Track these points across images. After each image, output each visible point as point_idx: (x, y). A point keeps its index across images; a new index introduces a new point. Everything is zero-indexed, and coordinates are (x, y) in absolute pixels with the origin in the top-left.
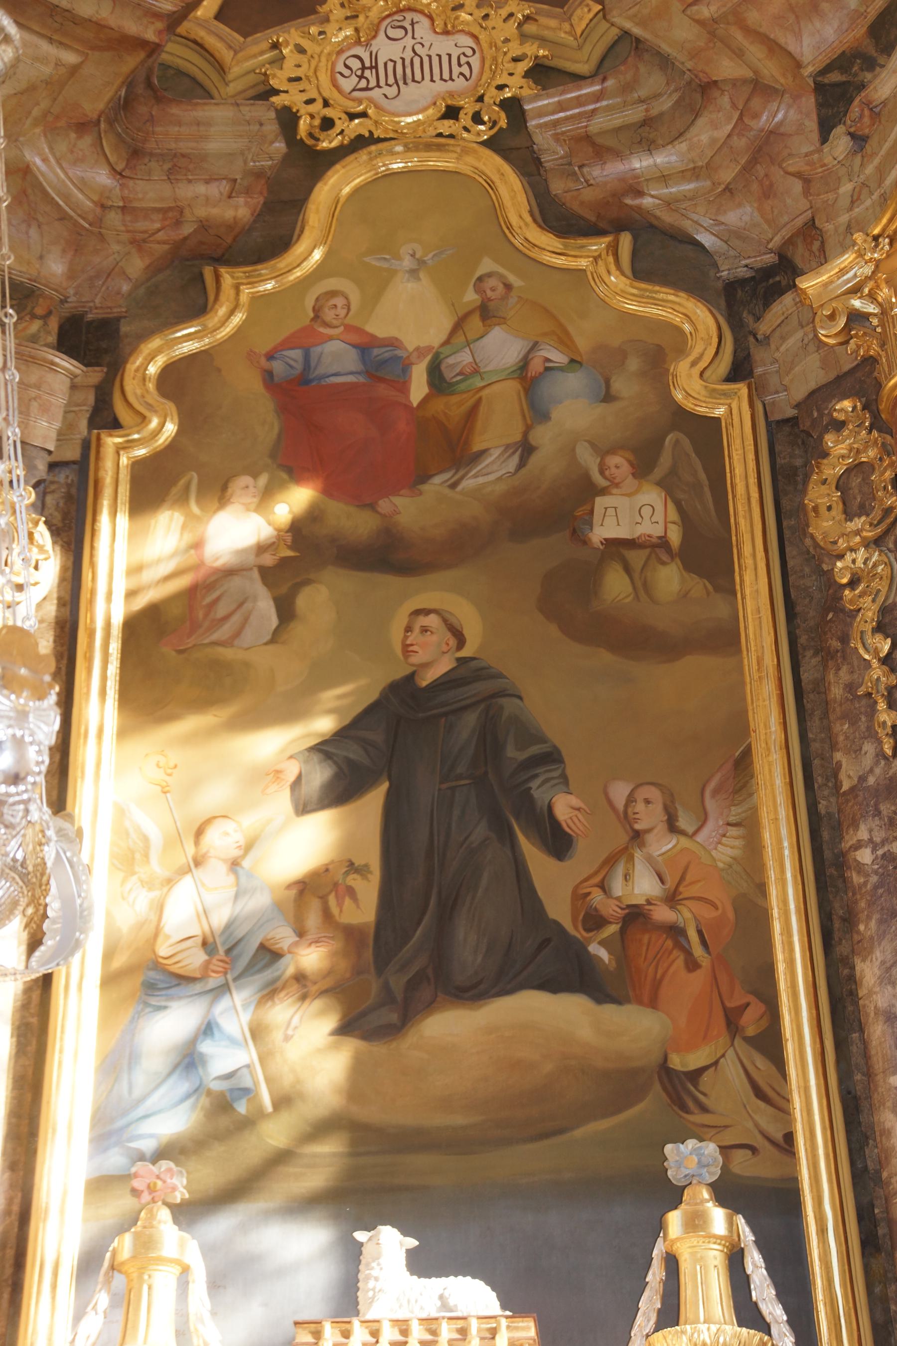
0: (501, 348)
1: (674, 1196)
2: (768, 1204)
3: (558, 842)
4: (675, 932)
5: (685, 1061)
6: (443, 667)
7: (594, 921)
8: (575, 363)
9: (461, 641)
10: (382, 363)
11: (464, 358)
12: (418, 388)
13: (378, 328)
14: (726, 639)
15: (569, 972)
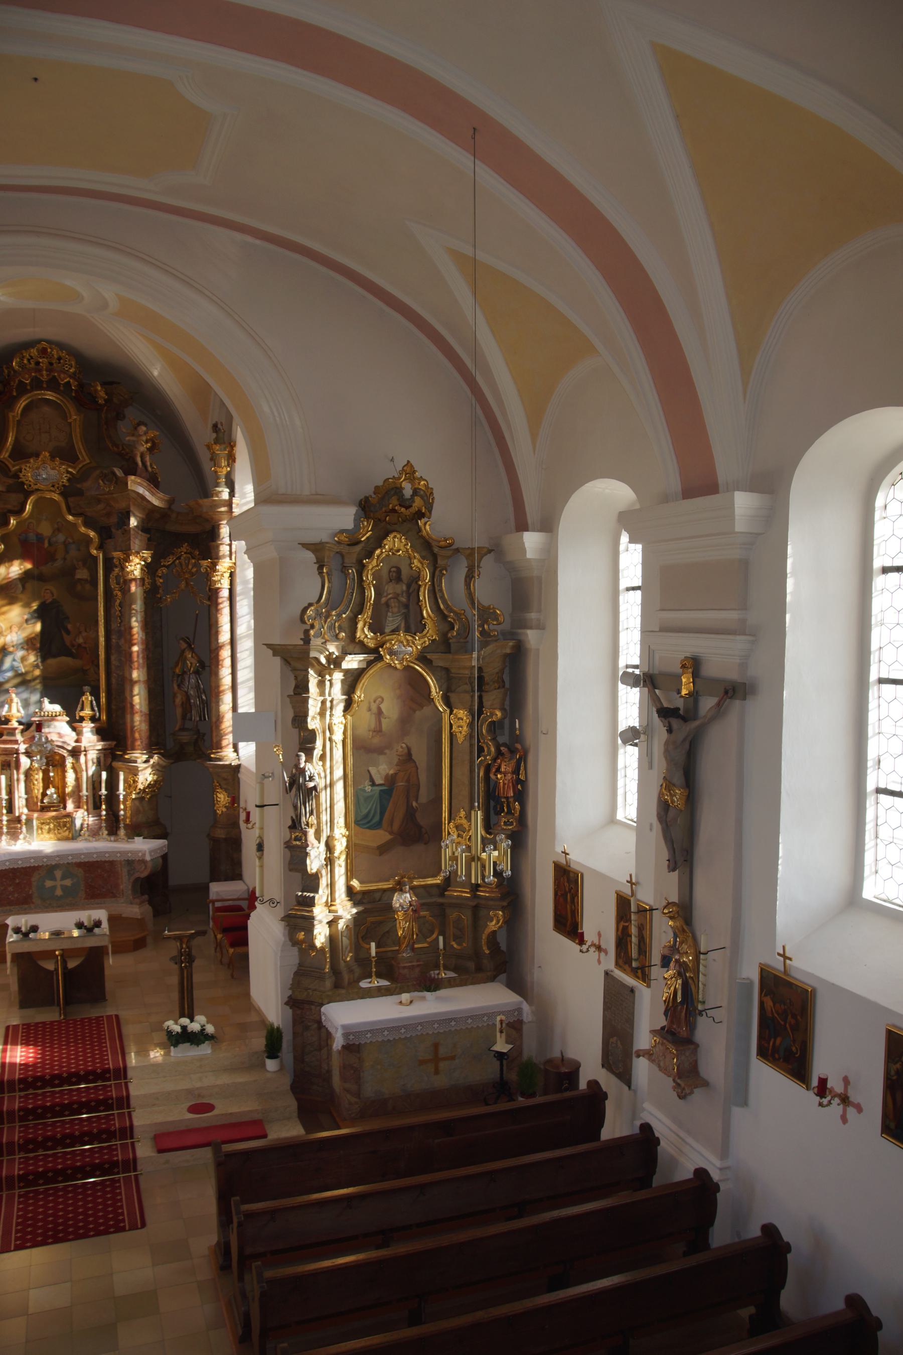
0: (61, 538)
1: (83, 694)
2: (96, 694)
4: (85, 648)
6: (50, 600)
7: (73, 646)
8: (74, 542)
9: (53, 595)
10: (40, 538)
11: (54, 539)
12: (46, 545)
13: (39, 531)
14: (96, 599)
15: (69, 654)
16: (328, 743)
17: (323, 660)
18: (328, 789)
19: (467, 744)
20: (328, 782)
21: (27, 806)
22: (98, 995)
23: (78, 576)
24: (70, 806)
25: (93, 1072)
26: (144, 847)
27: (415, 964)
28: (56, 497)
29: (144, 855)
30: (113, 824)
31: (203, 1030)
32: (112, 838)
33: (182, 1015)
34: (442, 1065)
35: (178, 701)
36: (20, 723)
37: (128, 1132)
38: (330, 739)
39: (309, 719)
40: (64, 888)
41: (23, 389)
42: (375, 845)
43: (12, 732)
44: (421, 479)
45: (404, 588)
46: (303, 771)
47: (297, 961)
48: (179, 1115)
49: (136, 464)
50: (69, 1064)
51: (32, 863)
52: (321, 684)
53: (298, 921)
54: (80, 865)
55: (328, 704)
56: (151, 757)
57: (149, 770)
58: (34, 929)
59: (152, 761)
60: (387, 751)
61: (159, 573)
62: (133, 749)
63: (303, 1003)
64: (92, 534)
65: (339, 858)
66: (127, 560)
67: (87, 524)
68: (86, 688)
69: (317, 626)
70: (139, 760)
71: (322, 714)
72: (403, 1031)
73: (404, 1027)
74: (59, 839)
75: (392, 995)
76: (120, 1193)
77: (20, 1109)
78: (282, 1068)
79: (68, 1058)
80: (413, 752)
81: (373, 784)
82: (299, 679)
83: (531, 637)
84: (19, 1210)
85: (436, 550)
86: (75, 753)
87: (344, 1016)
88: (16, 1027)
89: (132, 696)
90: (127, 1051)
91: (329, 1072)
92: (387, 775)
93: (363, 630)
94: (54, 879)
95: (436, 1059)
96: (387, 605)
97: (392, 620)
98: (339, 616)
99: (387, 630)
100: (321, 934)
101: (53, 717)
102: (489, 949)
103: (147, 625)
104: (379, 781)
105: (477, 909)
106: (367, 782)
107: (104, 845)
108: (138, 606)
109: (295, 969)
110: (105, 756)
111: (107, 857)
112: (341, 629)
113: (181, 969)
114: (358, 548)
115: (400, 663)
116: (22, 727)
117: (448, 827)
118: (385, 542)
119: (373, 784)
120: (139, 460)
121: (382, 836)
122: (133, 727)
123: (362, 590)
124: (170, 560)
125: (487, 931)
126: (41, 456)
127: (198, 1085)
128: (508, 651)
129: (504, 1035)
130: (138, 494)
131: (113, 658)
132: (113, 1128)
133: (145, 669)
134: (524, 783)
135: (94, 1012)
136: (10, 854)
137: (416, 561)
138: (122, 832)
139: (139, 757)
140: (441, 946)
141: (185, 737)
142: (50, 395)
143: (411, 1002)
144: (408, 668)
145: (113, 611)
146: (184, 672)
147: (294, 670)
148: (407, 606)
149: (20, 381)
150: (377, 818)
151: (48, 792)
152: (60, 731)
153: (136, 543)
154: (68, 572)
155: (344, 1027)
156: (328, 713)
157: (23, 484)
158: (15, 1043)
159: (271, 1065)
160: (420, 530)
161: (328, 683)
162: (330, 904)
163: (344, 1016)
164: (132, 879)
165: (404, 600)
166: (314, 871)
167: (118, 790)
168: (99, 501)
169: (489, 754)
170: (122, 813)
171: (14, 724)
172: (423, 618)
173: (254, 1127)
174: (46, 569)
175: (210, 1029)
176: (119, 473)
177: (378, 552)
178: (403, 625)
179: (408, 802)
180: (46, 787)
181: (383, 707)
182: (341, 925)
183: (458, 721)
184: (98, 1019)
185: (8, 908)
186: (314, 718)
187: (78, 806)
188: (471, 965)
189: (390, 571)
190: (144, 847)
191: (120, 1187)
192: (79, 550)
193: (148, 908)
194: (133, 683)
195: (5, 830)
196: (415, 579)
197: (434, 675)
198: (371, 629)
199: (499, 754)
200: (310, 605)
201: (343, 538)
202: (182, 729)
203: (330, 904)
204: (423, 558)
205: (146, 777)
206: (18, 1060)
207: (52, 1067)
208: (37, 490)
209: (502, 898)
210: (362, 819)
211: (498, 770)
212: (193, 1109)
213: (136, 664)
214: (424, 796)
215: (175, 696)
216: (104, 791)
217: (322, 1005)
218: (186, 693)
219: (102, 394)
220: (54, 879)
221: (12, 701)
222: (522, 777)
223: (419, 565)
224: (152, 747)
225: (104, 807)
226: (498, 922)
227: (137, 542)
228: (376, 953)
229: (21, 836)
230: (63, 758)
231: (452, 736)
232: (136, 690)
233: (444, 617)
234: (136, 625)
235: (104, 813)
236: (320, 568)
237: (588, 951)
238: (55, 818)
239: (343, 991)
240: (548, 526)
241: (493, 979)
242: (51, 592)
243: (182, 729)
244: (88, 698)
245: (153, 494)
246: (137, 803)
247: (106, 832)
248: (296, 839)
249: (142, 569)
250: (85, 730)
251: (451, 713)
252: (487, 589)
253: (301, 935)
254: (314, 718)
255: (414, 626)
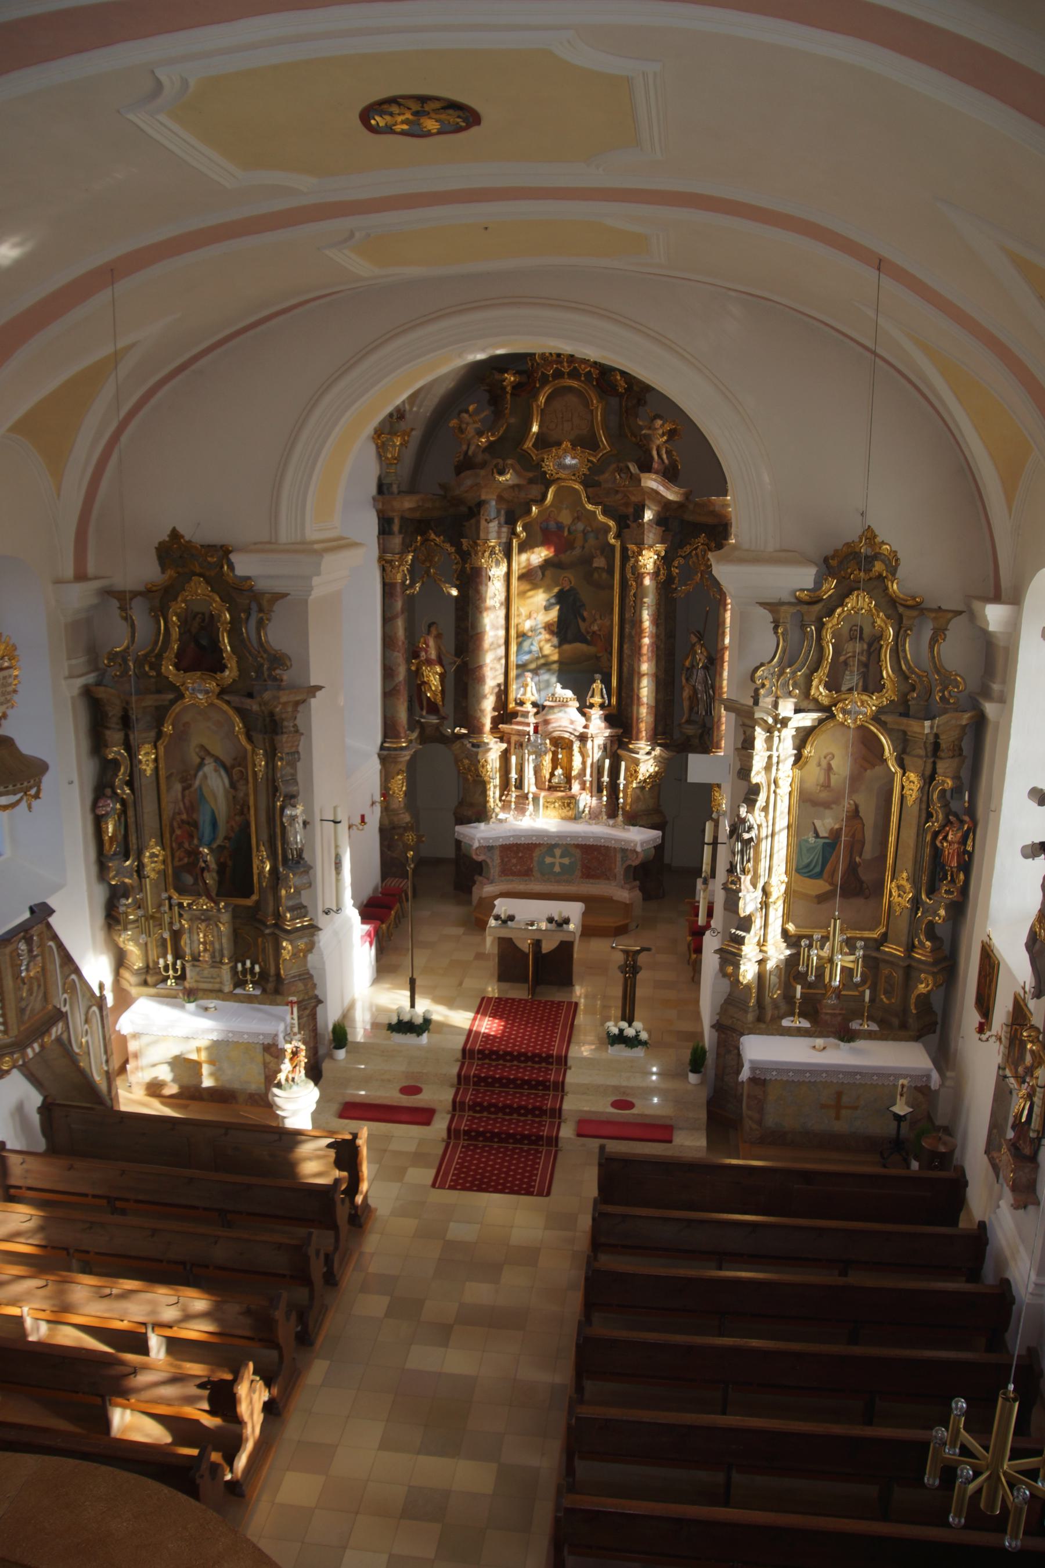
0: (580, 526)
1: (594, 681)
2: (607, 682)
3: (584, 620)
5: (599, 655)
7: (588, 633)
10: (560, 527)
12: (566, 533)
13: (560, 519)
14: (612, 587)
15: (583, 639)
16: (772, 796)
17: (770, 721)
18: (769, 839)
19: (916, 808)
20: (770, 832)
21: (536, 784)
22: (567, 982)
23: (595, 565)
24: (576, 787)
25: (539, 1055)
26: (640, 837)
27: (837, 1012)
28: (577, 486)
29: (636, 845)
30: (612, 810)
31: (637, 1036)
32: (611, 822)
33: (623, 1019)
34: (844, 1112)
35: (686, 694)
36: (535, 704)
37: (557, 1113)
38: (775, 792)
39: (753, 774)
40: (562, 865)
41: (545, 380)
42: (814, 893)
43: (525, 714)
44: (883, 543)
45: (865, 647)
46: (743, 821)
47: (728, 990)
48: (602, 1106)
49: (652, 457)
50: (522, 1043)
51: (534, 840)
52: (769, 740)
53: (730, 958)
54: (577, 846)
55: (775, 760)
56: (653, 749)
57: (652, 761)
58: (511, 918)
59: (654, 753)
60: (834, 806)
61: (676, 563)
62: (637, 739)
63: (729, 1032)
64: (611, 523)
65: (775, 903)
66: (640, 554)
67: (605, 513)
68: (598, 676)
69: (767, 683)
70: (642, 752)
71: (768, 768)
72: (808, 1075)
73: (809, 1071)
74: (562, 818)
75: (811, 1036)
76: (539, 1163)
77: (474, 1076)
78: (702, 1082)
79: (523, 1038)
80: (861, 809)
81: (817, 836)
82: (748, 733)
83: (990, 709)
84: (459, 1158)
85: (901, 609)
86: (583, 738)
87: (759, 1050)
88: (490, 999)
89: (639, 689)
90: (573, 1039)
91: (742, 1095)
92: (832, 830)
93: (817, 688)
94: (554, 856)
95: (838, 1106)
96: (846, 663)
97: (852, 678)
98: (794, 673)
99: (844, 688)
100: (748, 971)
101: (563, 704)
102: (916, 1008)
103: (656, 621)
104: (823, 833)
105: (909, 972)
106: (811, 834)
107: (601, 830)
108: (649, 600)
109: (725, 996)
110: (612, 741)
111: (602, 842)
112: (795, 686)
113: (626, 980)
114: (817, 608)
115: (855, 720)
116: (535, 710)
117: (890, 886)
118: (847, 600)
119: (817, 836)
120: (655, 453)
121: (821, 886)
122: (638, 719)
123: (821, 650)
124: (688, 549)
125: (916, 993)
126: (564, 446)
127: (624, 1083)
128: (964, 722)
129: (904, 1098)
130: (652, 489)
131: (625, 646)
132: (544, 1108)
133: (654, 662)
134: (971, 855)
135: (558, 996)
136: (514, 830)
137: (879, 621)
138: (620, 818)
139: (643, 746)
140: (867, 998)
141: (690, 730)
142: (574, 384)
143: (824, 1048)
144: (862, 728)
145: (627, 601)
146: (693, 666)
147: (744, 725)
148: (866, 665)
149: (543, 373)
150: (818, 869)
151: (556, 773)
152: (568, 719)
153: (650, 537)
154: (586, 561)
155: (751, 1061)
156: (774, 768)
157: (545, 473)
158: (484, 1014)
159: (693, 1078)
160: (887, 588)
161: (776, 739)
162: (761, 944)
163: (759, 1050)
164: (624, 866)
165: (864, 659)
166: (747, 913)
167: (618, 778)
168: (617, 492)
169: (937, 821)
170: (621, 800)
171: (528, 707)
172: (882, 678)
173: (660, 1130)
174: (565, 558)
175: (644, 1036)
176: (633, 468)
177: (839, 610)
178: (861, 684)
179: (851, 857)
180: (554, 768)
181: (833, 763)
182: (770, 965)
183: (909, 784)
184: (560, 1004)
185: (511, 878)
186: (758, 773)
187: (583, 789)
188: (896, 1022)
189: (851, 630)
190: (640, 837)
191: (540, 1158)
192: (597, 538)
193: (638, 894)
194: (641, 676)
195: (513, 806)
196: (878, 638)
197: (889, 735)
198: (827, 687)
199: (948, 823)
200: (762, 665)
201: (804, 595)
202: (689, 722)
203: (761, 944)
204: (888, 617)
205: (647, 767)
206: (483, 1030)
207: (506, 1045)
208: (558, 479)
209: (935, 963)
210: (806, 865)
211: (945, 838)
212: (616, 1104)
213: (645, 658)
214: (869, 851)
215: (682, 688)
216: (606, 779)
217: (742, 1034)
218: (694, 686)
219: (623, 383)
220: (554, 856)
221: (527, 685)
222: (969, 849)
223: (883, 625)
224: (654, 740)
225: (605, 793)
226: (927, 985)
227: (651, 535)
228: (799, 997)
229: (528, 813)
230: (572, 742)
231: (902, 797)
232: (645, 682)
233: (907, 678)
234: (646, 616)
235: (605, 799)
236: (776, 628)
237: (987, 1040)
238: (562, 798)
239: (763, 1026)
240: (1015, 598)
241: (916, 1038)
242: (570, 579)
243: (689, 722)
244: (598, 686)
245: (668, 489)
246: (638, 791)
247: (605, 817)
248: (733, 882)
249: (655, 563)
250: (593, 717)
251: (904, 775)
252: (954, 652)
253: (730, 969)
254: (758, 773)
255: (871, 684)
